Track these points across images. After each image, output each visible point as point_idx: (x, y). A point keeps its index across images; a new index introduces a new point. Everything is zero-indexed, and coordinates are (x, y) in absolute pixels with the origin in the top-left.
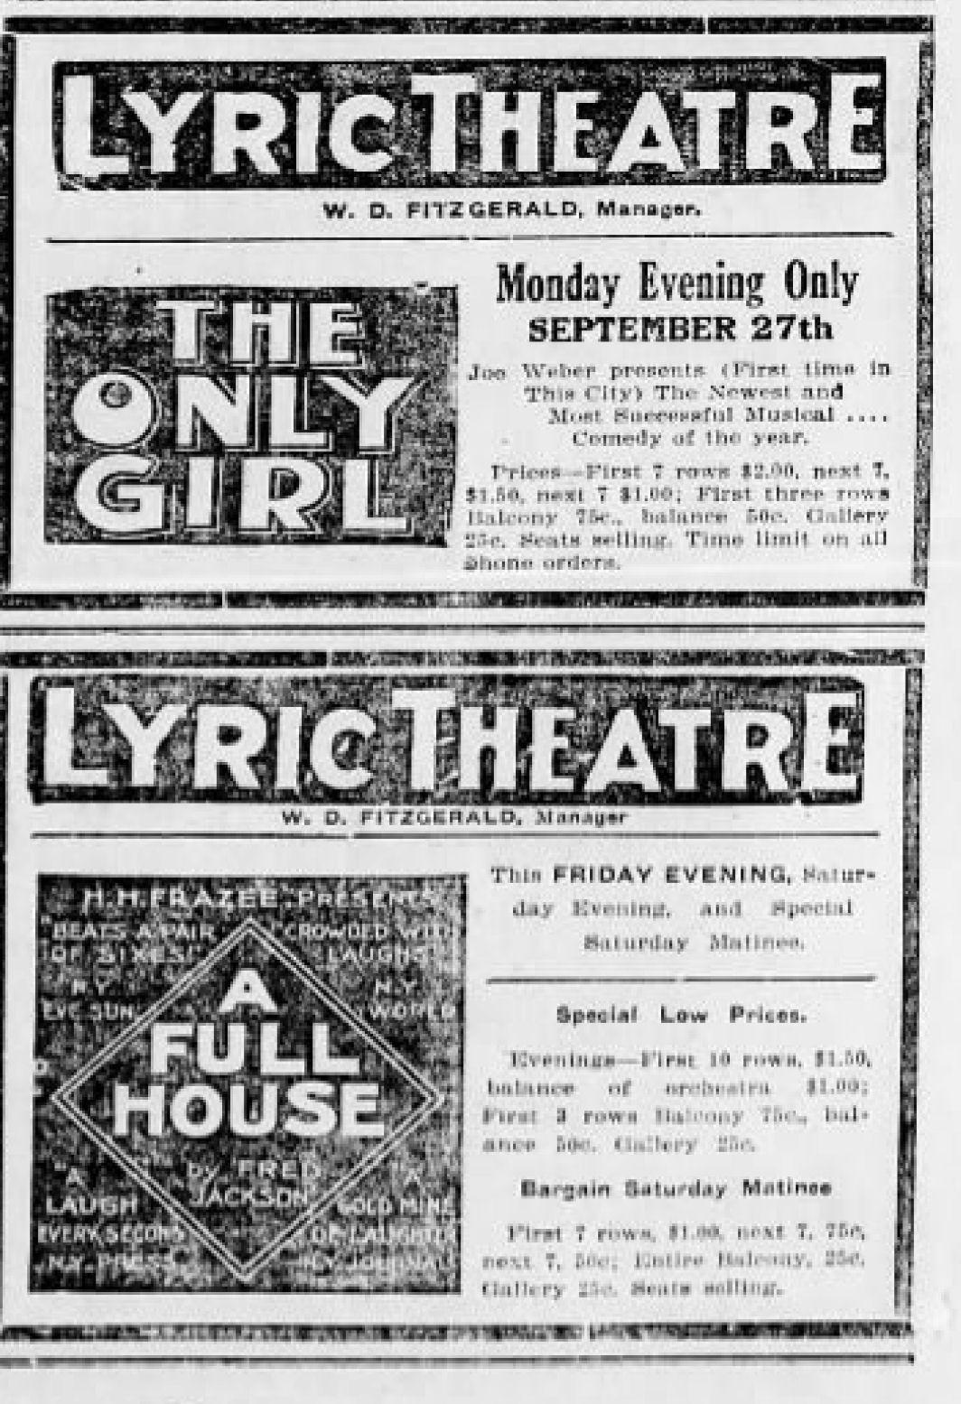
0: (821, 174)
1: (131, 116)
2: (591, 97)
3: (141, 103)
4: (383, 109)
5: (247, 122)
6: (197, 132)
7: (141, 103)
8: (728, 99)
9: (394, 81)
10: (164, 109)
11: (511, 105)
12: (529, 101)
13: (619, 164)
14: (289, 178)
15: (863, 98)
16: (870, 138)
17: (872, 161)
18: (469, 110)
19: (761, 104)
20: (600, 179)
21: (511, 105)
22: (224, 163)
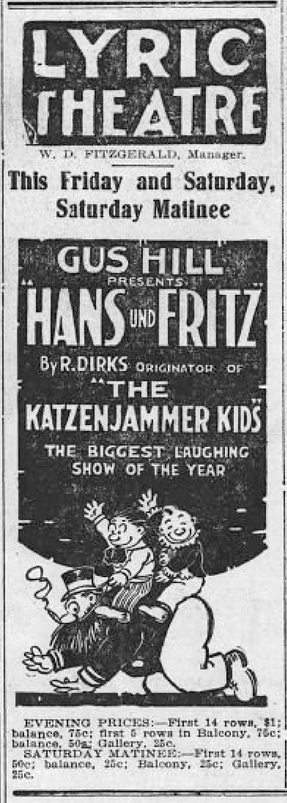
8: (197, 91)
13: (139, 132)
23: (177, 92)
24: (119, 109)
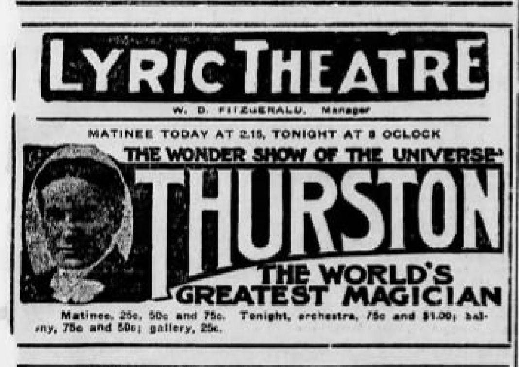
0: (454, 93)
1: (85, 60)
2: (329, 53)
3: (90, 55)
4: (219, 59)
5: (147, 65)
6: (120, 72)
7: (90, 55)
8: (401, 54)
9: (224, 42)
10: (103, 56)
11: (286, 57)
12: (296, 55)
14: (168, 95)
15: (474, 53)
16: (480, 74)
17: (479, 86)
18: (265, 59)
19: (420, 57)
20: (335, 97)
21: (286, 57)
22: (134, 87)
23: (382, 54)
24: (326, 68)
